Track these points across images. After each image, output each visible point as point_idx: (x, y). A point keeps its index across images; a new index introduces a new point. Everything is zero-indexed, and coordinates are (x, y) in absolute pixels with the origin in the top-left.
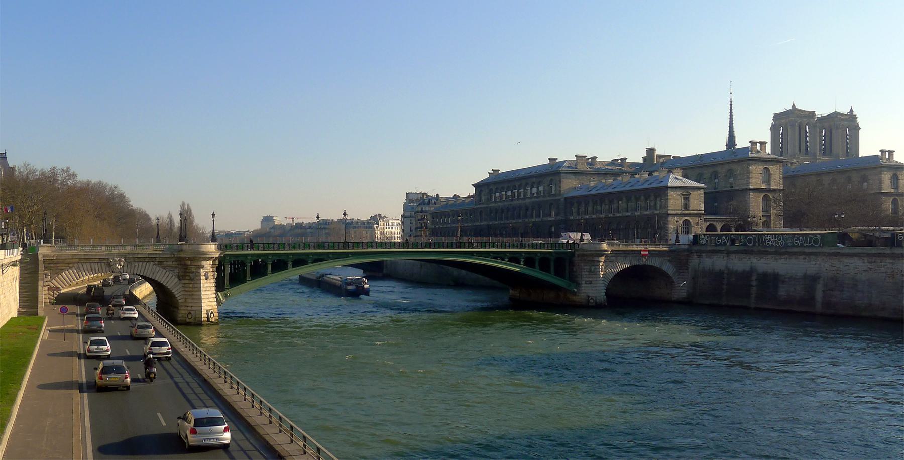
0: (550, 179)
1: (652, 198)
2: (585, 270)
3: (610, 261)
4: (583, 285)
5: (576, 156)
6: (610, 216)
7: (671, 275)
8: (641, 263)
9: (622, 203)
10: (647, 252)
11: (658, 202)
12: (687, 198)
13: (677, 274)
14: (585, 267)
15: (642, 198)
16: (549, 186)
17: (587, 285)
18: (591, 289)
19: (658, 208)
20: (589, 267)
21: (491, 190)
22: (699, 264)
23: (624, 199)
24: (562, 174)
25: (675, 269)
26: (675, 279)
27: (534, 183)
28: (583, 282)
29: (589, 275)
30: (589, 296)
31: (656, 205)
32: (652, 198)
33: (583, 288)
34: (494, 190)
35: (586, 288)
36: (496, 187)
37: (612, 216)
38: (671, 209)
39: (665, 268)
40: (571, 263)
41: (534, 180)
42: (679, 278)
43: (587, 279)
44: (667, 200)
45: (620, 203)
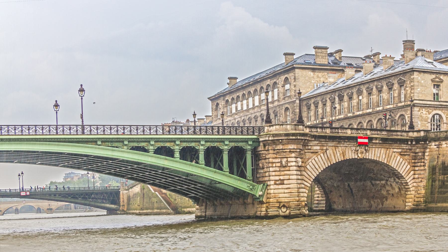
0: (283, 78)
1: (396, 86)
2: (274, 165)
3: (312, 153)
4: (272, 187)
5: (315, 48)
6: (349, 115)
7: (403, 175)
8: (360, 155)
9: (363, 98)
10: (366, 141)
11: (403, 91)
12: (437, 86)
13: (412, 172)
14: (274, 160)
15: (385, 88)
16: (283, 86)
17: (276, 187)
18: (282, 191)
19: (403, 99)
20: (279, 160)
21: (227, 101)
22: (438, 157)
23: (365, 91)
24: (296, 70)
25: (409, 166)
26: (409, 178)
27: (268, 85)
28: (272, 183)
29: (279, 171)
30: (280, 202)
31: (400, 94)
32: (396, 86)
33: (272, 191)
34: (230, 100)
35: (276, 191)
36: (231, 97)
37: (351, 115)
38: (418, 99)
39: (393, 164)
40: (256, 156)
41: (268, 82)
42: (414, 178)
43: (277, 178)
44: (412, 88)
45: (360, 98)
